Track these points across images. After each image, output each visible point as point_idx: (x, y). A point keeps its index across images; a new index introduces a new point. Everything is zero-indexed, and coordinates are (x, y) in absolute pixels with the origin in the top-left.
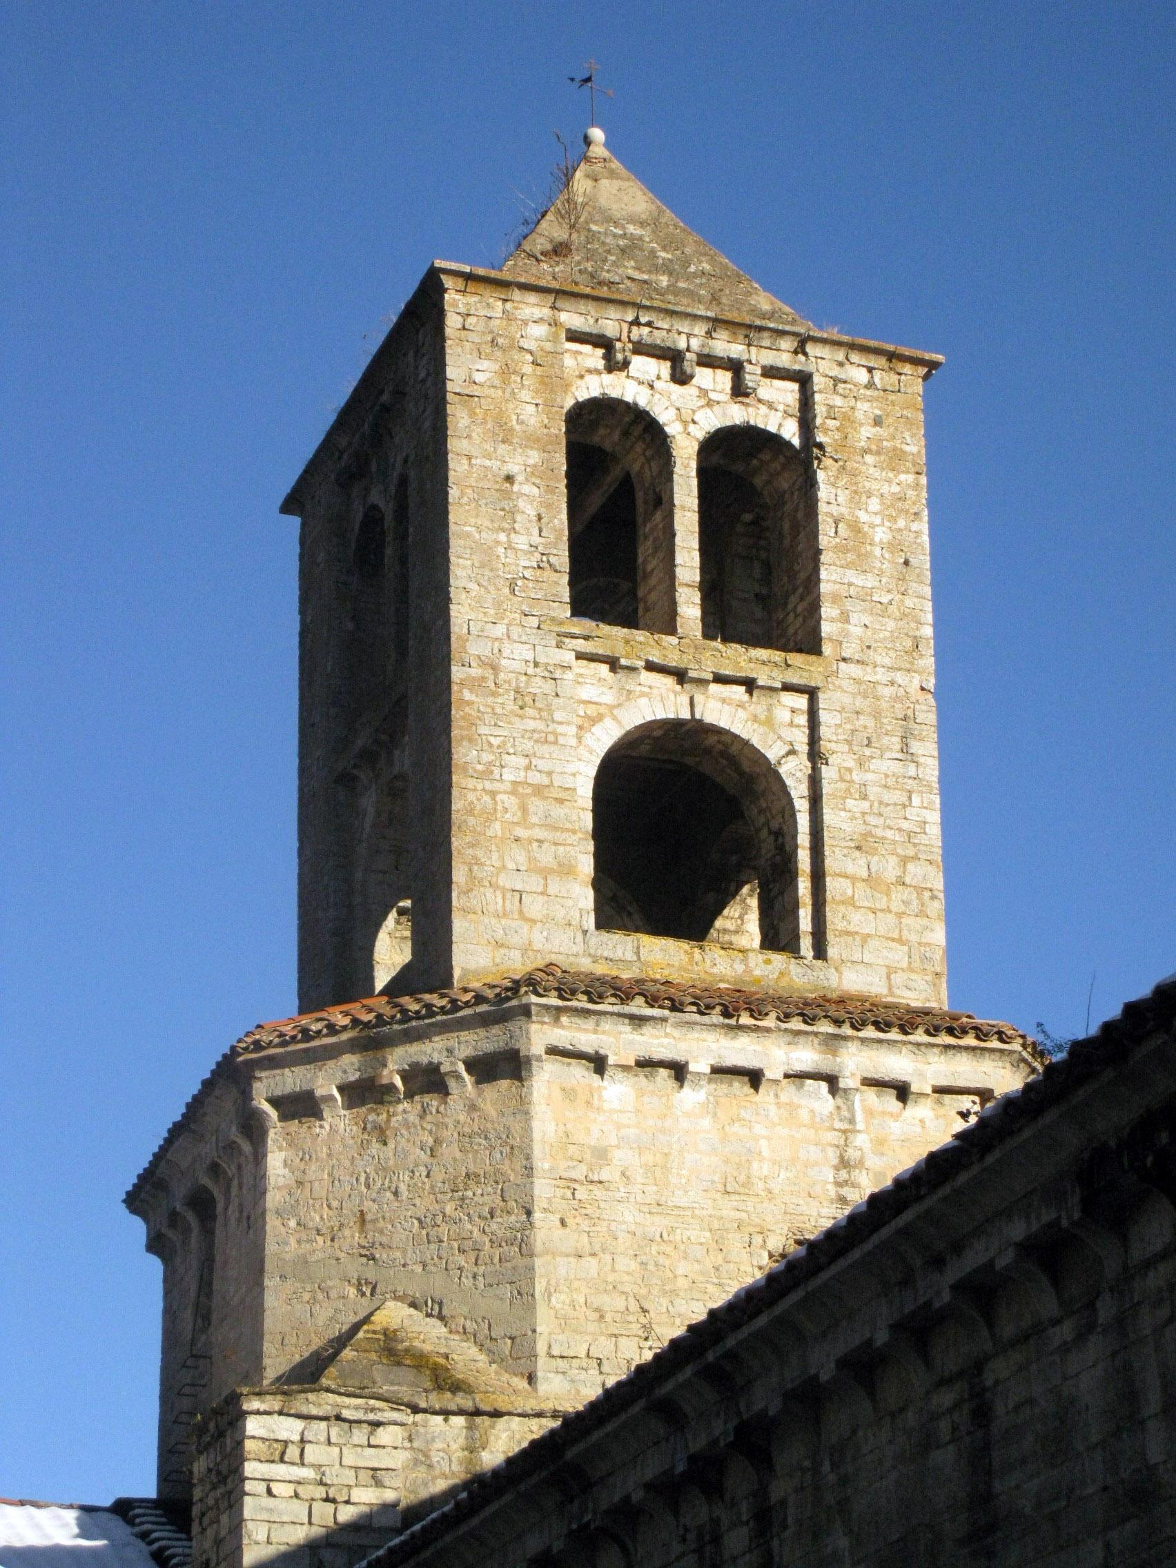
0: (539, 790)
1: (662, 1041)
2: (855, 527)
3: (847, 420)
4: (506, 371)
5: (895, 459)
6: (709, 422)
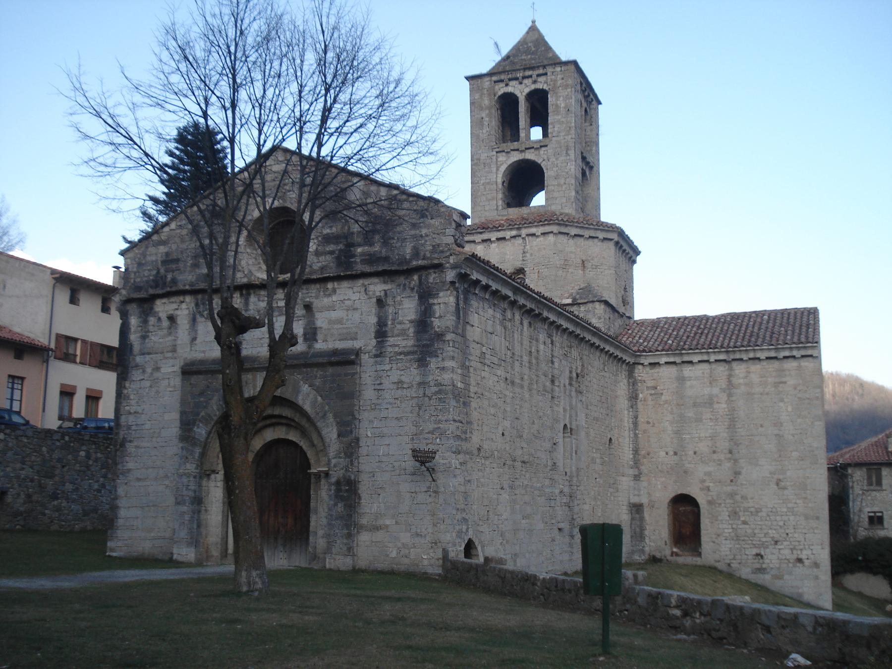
0: (488, 183)
1: (485, 236)
2: (557, 106)
3: (556, 81)
4: (482, 94)
5: (566, 86)
6: (527, 90)
